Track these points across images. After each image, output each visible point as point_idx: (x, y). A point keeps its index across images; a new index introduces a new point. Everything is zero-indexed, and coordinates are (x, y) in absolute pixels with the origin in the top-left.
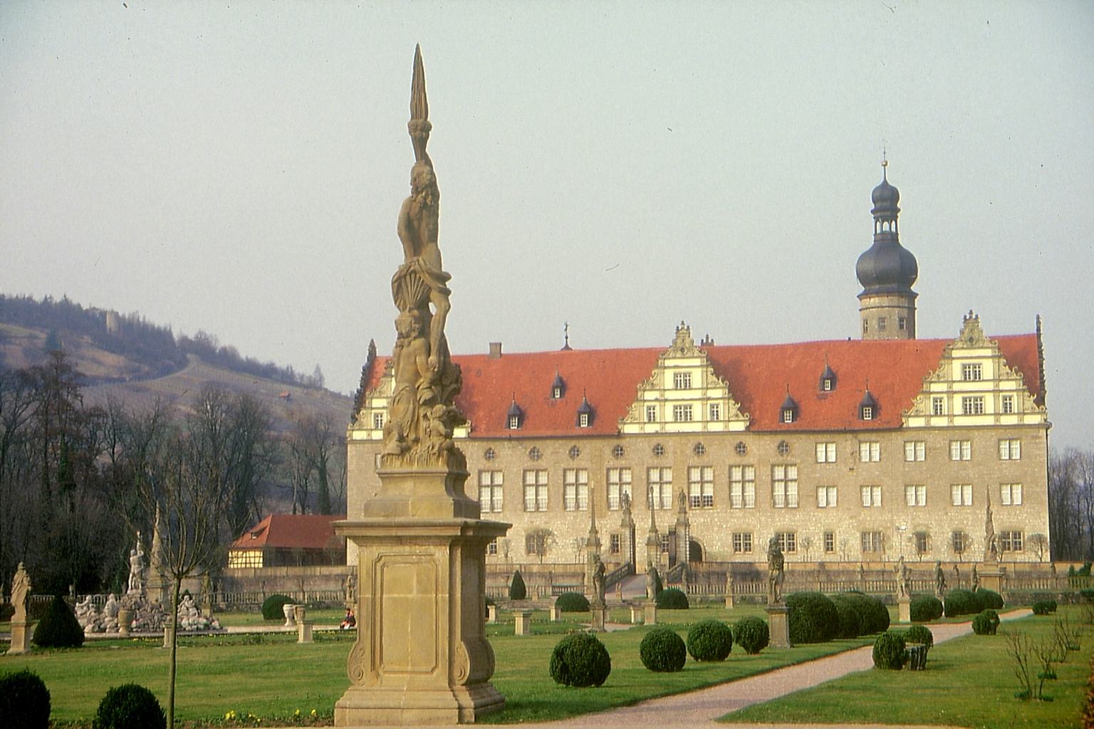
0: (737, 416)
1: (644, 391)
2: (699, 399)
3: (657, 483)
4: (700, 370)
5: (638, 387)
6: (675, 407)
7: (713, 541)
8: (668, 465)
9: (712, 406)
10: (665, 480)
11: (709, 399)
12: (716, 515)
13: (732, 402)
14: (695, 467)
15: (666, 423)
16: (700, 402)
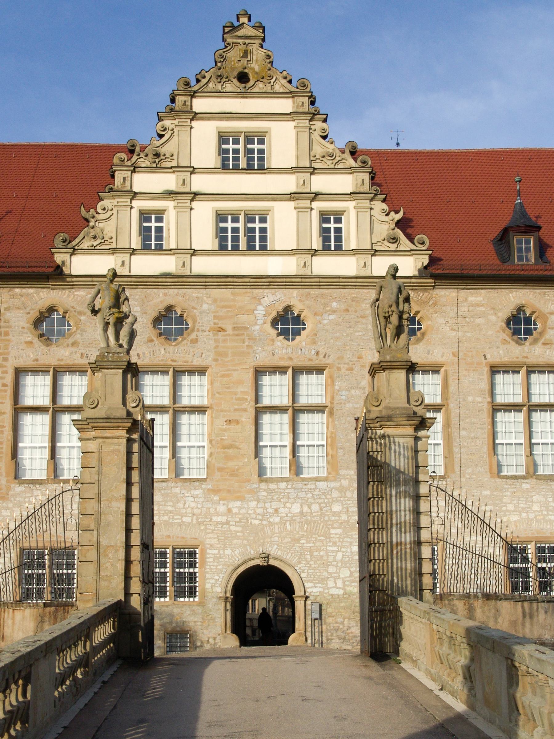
0: (394, 240)
1: (134, 171)
2: (293, 196)
3: (162, 409)
4: (289, 126)
5: (116, 160)
6: (221, 217)
7: (326, 565)
8: (197, 362)
9: (324, 218)
10: (185, 402)
11: (316, 196)
12: (335, 494)
13: (379, 206)
14: (274, 371)
15: (194, 253)
16: (292, 204)
